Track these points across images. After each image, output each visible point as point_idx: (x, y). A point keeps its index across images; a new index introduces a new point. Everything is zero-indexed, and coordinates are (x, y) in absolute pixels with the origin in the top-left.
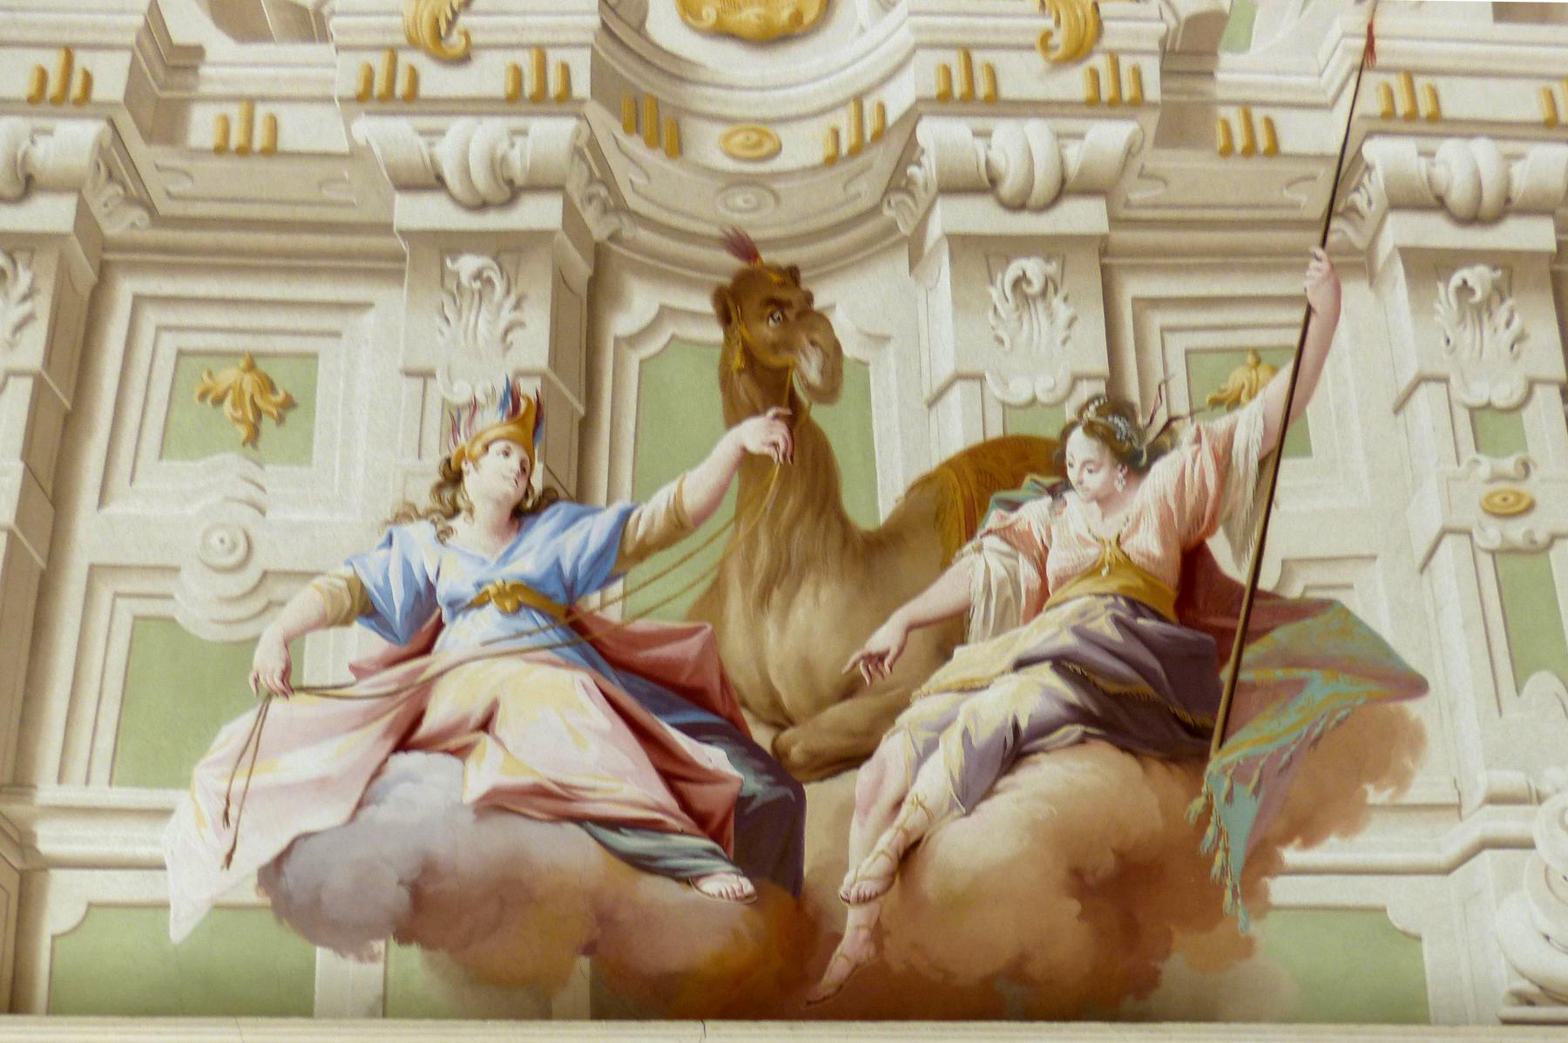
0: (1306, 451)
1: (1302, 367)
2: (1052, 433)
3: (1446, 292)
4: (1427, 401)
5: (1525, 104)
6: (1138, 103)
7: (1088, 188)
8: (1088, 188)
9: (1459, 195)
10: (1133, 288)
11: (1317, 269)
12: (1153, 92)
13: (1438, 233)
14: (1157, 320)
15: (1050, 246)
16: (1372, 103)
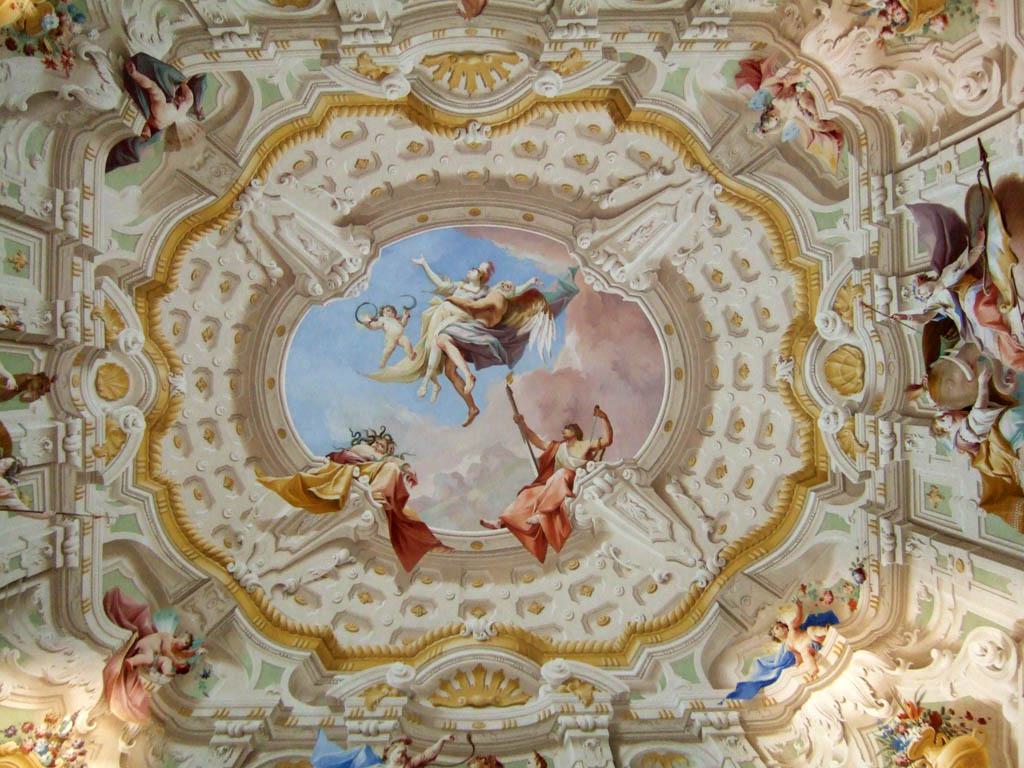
0: (10, 516)
1: (30, 513)
2: (13, 454)
3: (47, 545)
4: (21, 545)
5: (87, 554)
6: (85, 467)
7: (68, 457)
8: (68, 457)
9: (67, 543)
10: (46, 470)
11: (51, 513)
12: (88, 470)
13: (59, 540)
14: (39, 477)
15: (55, 451)
16: (86, 520)
